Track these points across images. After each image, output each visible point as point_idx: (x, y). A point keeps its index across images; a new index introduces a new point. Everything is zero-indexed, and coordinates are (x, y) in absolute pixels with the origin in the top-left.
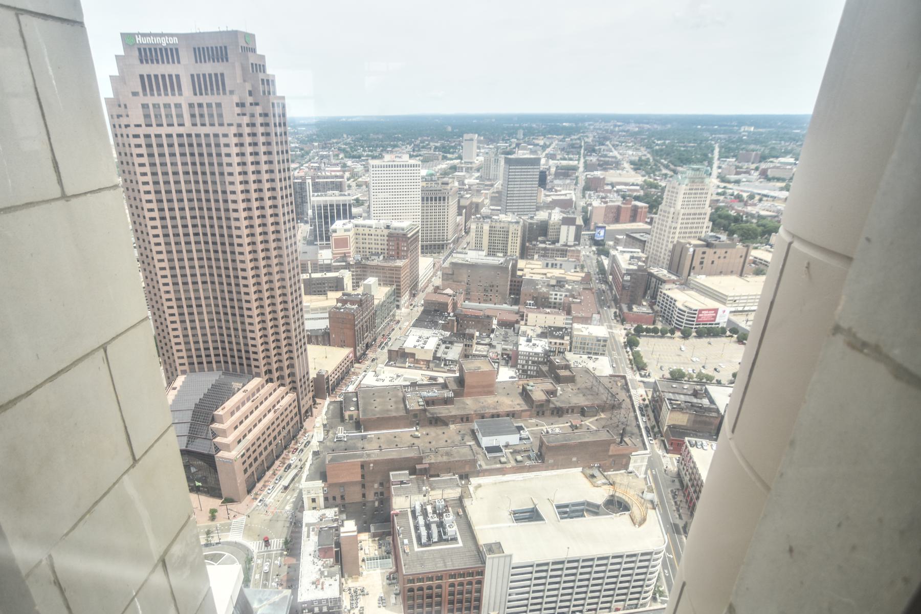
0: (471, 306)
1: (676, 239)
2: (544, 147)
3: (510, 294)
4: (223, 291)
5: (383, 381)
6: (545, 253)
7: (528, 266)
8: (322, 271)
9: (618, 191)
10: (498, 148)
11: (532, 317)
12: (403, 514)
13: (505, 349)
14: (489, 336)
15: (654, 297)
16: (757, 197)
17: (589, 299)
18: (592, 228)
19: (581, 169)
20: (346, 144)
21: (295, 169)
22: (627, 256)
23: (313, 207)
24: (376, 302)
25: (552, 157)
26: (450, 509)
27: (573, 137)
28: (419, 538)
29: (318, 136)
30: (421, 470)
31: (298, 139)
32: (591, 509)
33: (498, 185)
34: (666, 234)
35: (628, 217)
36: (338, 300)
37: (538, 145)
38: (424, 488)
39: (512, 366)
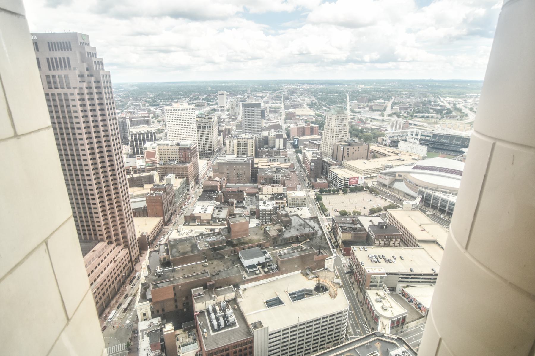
0: (231, 186)
1: (334, 143)
4: (75, 190)
5: (183, 234)
6: (268, 154)
8: (139, 173)
12: (202, 313)
13: (253, 209)
14: (242, 202)
15: (327, 173)
16: (370, 120)
19: (283, 109)
20: (149, 98)
21: (118, 113)
22: (311, 153)
23: (132, 135)
24: (175, 188)
25: (267, 102)
26: (230, 306)
27: (277, 92)
28: (212, 326)
29: (132, 94)
30: (210, 285)
31: (119, 95)
33: (240, 118)
34: (329, 140)
36: (151, 189)
38: (213, 296)
39: (257, 218)
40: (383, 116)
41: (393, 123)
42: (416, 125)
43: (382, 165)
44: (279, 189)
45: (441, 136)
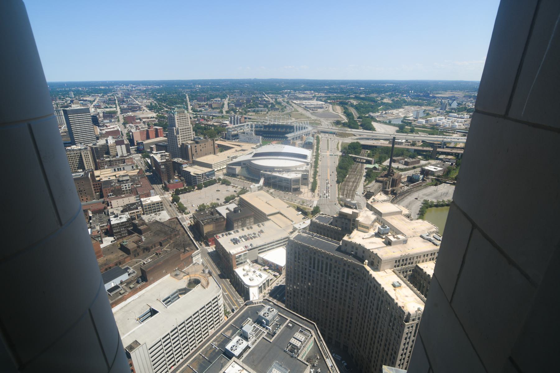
2: (91, 102)
3: (96, 192)
6: (111, 164)
7: (102, 173)
9: (144, 122)
10: (57, 104)
11: (114, 203)
13: (103, 226)
16: (211, 117)
17: (146, 182)
18: (136, 144)
22: (159, 155)
32: (184, 291)
35: (154, 135)
37: (86, 100)
40: (222, 113)
41: (231, 119)
42: (250, 119)
43: (228, 157)
44: (132, 199)
45: (269, 126)
